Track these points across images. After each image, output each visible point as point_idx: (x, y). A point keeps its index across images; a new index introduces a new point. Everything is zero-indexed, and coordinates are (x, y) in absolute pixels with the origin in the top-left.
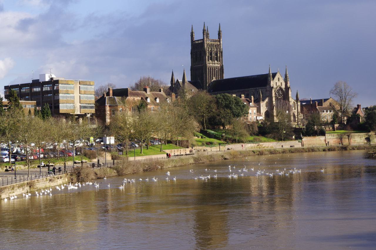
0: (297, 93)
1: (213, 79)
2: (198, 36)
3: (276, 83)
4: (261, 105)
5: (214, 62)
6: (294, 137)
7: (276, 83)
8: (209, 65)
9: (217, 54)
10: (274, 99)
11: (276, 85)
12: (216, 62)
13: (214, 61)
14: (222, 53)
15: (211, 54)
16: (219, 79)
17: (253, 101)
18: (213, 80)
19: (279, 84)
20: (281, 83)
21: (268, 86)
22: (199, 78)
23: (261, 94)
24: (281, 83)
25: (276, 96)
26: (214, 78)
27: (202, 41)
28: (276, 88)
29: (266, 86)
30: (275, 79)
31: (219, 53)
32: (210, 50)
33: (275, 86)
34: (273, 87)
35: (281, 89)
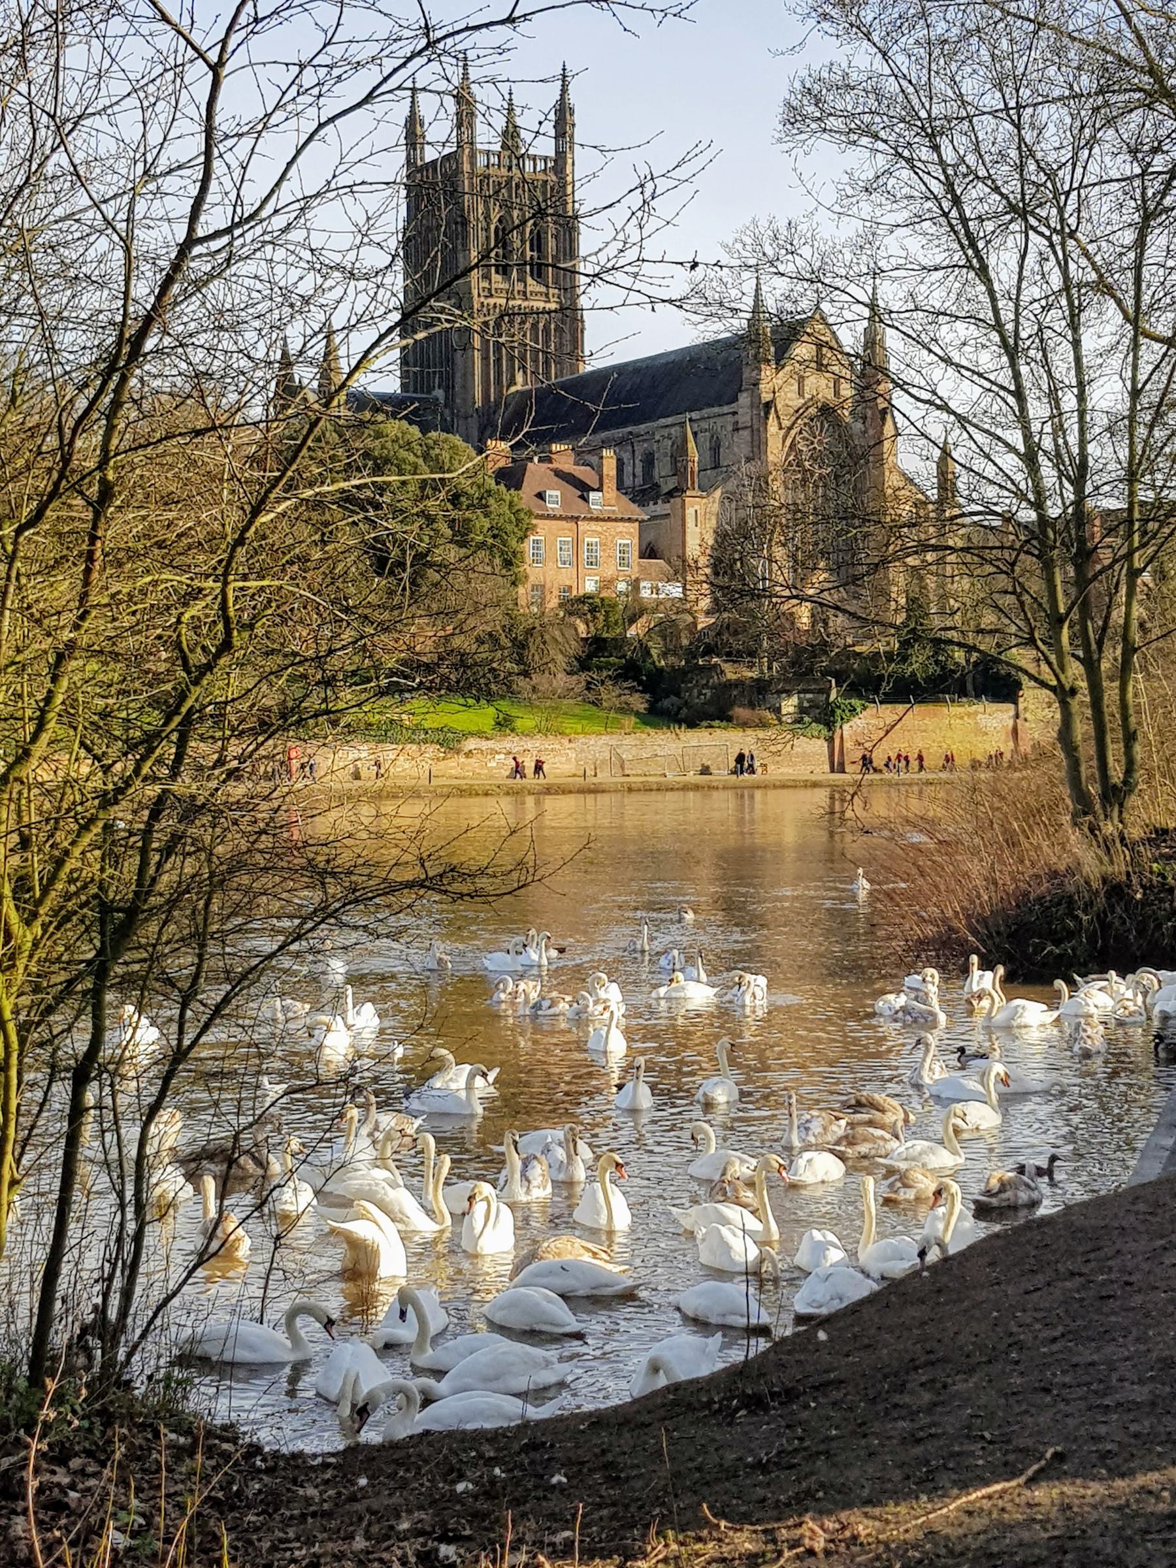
1: (512, 382)
4: (690, 512)
5: (519, 286)
6: (789, 705)
8: (492, 301)
11: (801, 393)
12: (532, 285)
13: (522, 280)
17: (610, 484)
18: (513, 389)
19: (819, 386)
21: (744, 399)
23: (691, 444)
26: (519, 377)
29: (735, 399)
31: (556, 237)
32: (495, 217)
34: (768, 406)
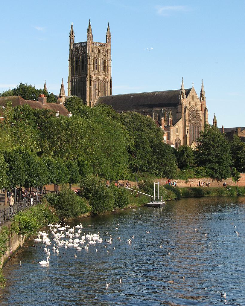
0: (215, 117)
2: (80, 38)
3: (190, 102)
4: (171, 130)
7: (190, 102)
8: (95, 76)
9: (103, 63)
10: (187, 123)
14: (110, 60)
15: (96, 62)
16: (107, 95)
19: (193, 104)
20: (196, 103)
22: (79, 93)
24: (196, 103)
25: (189, 120)
26: (100, 94)
27: (86, 44)
28: (190, 109)
30: (189, 96)
33: (188, 107)
35: (196, 110)
